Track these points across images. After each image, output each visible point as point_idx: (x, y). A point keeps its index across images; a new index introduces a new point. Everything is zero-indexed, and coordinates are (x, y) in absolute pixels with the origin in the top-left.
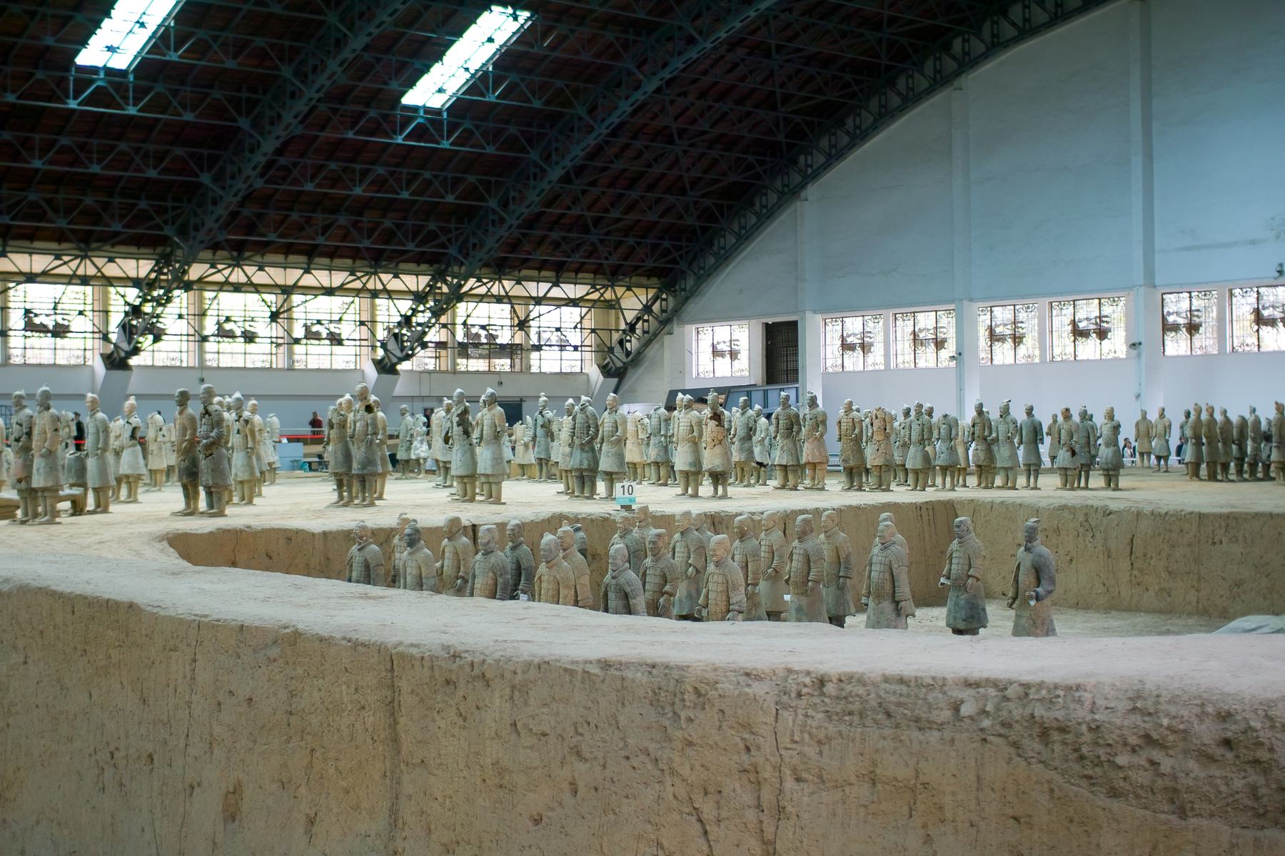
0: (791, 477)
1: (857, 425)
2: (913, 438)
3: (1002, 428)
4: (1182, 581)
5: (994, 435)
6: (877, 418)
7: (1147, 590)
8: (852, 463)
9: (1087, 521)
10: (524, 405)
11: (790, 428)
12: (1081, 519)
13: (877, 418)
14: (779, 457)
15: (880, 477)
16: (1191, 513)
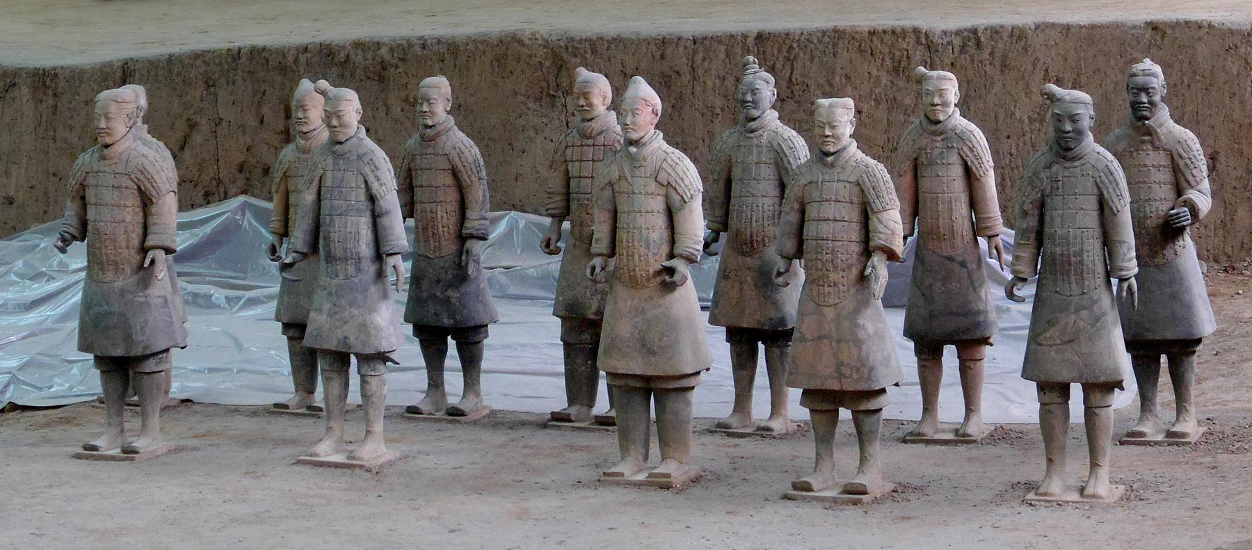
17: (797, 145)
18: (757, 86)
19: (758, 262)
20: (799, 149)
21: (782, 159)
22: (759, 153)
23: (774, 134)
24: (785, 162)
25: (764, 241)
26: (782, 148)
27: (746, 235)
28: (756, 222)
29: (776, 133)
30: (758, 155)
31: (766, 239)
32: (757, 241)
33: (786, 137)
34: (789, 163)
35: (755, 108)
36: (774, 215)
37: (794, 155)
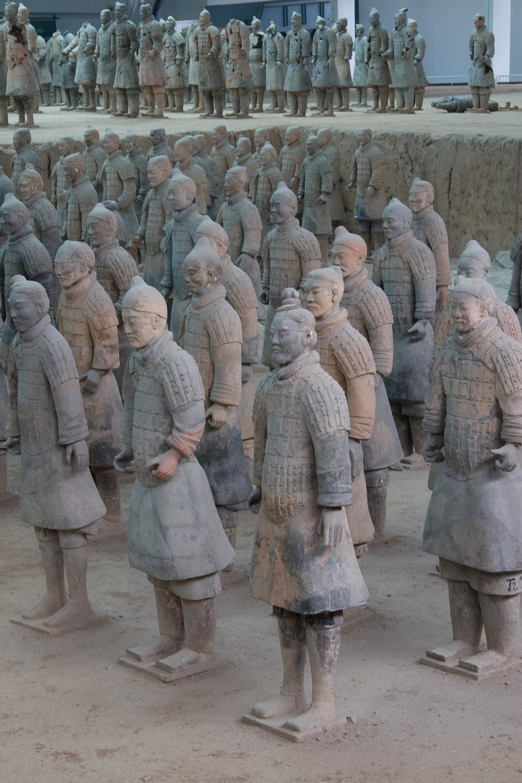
0: (130, 102)
1: (214, 42)
2: (291, 56)
3: (397, 42)
4: (500, 222)
5: (389, 51)
6: (231, 33)
7: (465, 232)
8: (210, 86)
9: (407, 152)
10: (58, 22)
11: (126, 45)
12: (401, 149)
13: (231, 33)
14: (120, 82)
15: (238, 102)
16: (511, 142)
17: (326, 398)
18: (286, 327)
19: (283, 533)
20: (329, 404)
21: (308, 414)
22: (288, 405)
23: (303, 383)
24: (312, 418)
25: (288, 508)
26: (308, 401)
27: (271, 500)
28: (280, 486)
29: (306, 382)
30: (286, 408)
31: (291, 507)
32: (282, 509)
33: (315, 388)
34: (315, 419)
35: (282, 352)
36: (301, 479)
37: (322, 411)
